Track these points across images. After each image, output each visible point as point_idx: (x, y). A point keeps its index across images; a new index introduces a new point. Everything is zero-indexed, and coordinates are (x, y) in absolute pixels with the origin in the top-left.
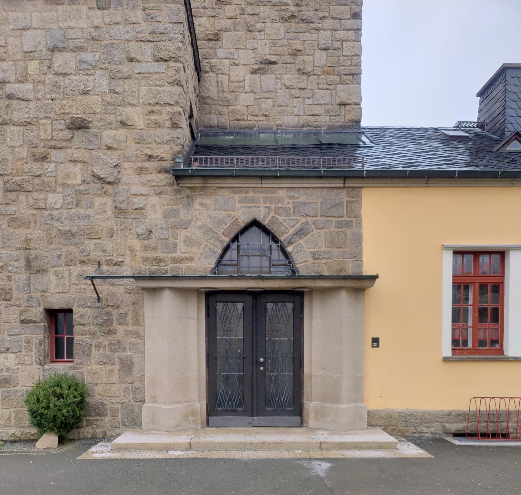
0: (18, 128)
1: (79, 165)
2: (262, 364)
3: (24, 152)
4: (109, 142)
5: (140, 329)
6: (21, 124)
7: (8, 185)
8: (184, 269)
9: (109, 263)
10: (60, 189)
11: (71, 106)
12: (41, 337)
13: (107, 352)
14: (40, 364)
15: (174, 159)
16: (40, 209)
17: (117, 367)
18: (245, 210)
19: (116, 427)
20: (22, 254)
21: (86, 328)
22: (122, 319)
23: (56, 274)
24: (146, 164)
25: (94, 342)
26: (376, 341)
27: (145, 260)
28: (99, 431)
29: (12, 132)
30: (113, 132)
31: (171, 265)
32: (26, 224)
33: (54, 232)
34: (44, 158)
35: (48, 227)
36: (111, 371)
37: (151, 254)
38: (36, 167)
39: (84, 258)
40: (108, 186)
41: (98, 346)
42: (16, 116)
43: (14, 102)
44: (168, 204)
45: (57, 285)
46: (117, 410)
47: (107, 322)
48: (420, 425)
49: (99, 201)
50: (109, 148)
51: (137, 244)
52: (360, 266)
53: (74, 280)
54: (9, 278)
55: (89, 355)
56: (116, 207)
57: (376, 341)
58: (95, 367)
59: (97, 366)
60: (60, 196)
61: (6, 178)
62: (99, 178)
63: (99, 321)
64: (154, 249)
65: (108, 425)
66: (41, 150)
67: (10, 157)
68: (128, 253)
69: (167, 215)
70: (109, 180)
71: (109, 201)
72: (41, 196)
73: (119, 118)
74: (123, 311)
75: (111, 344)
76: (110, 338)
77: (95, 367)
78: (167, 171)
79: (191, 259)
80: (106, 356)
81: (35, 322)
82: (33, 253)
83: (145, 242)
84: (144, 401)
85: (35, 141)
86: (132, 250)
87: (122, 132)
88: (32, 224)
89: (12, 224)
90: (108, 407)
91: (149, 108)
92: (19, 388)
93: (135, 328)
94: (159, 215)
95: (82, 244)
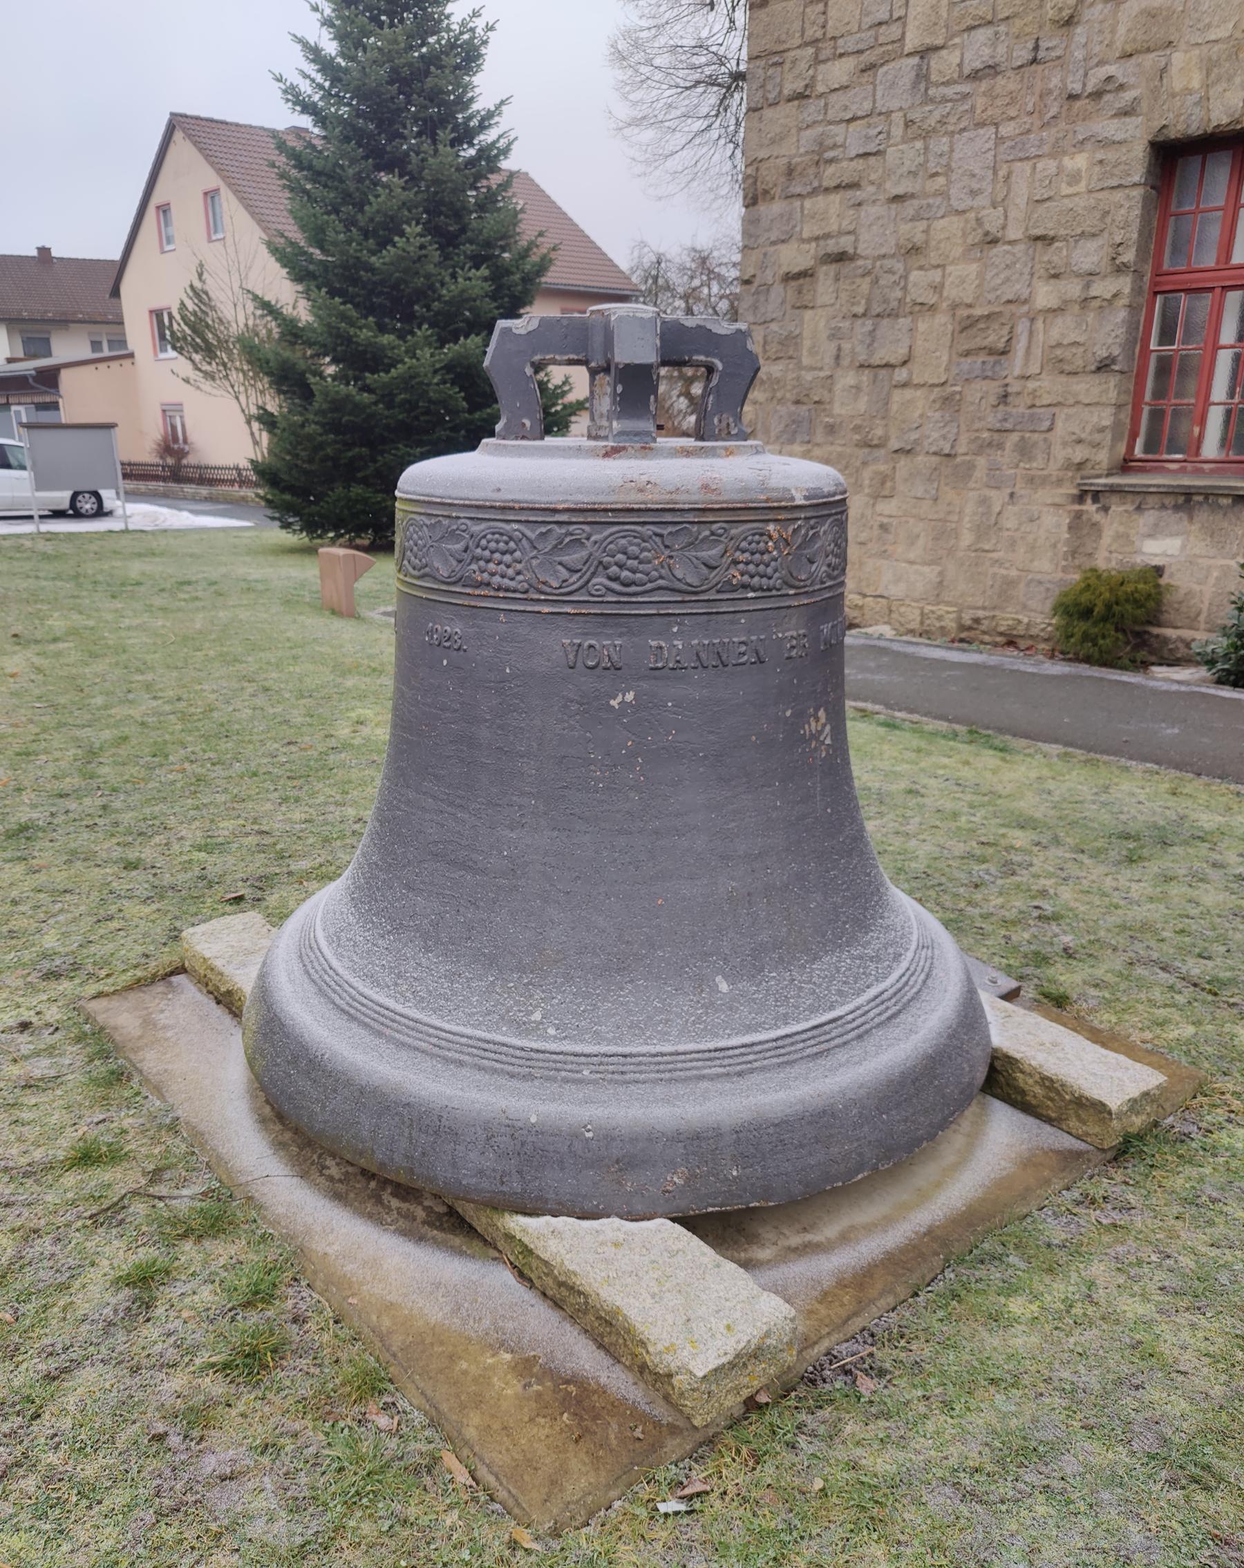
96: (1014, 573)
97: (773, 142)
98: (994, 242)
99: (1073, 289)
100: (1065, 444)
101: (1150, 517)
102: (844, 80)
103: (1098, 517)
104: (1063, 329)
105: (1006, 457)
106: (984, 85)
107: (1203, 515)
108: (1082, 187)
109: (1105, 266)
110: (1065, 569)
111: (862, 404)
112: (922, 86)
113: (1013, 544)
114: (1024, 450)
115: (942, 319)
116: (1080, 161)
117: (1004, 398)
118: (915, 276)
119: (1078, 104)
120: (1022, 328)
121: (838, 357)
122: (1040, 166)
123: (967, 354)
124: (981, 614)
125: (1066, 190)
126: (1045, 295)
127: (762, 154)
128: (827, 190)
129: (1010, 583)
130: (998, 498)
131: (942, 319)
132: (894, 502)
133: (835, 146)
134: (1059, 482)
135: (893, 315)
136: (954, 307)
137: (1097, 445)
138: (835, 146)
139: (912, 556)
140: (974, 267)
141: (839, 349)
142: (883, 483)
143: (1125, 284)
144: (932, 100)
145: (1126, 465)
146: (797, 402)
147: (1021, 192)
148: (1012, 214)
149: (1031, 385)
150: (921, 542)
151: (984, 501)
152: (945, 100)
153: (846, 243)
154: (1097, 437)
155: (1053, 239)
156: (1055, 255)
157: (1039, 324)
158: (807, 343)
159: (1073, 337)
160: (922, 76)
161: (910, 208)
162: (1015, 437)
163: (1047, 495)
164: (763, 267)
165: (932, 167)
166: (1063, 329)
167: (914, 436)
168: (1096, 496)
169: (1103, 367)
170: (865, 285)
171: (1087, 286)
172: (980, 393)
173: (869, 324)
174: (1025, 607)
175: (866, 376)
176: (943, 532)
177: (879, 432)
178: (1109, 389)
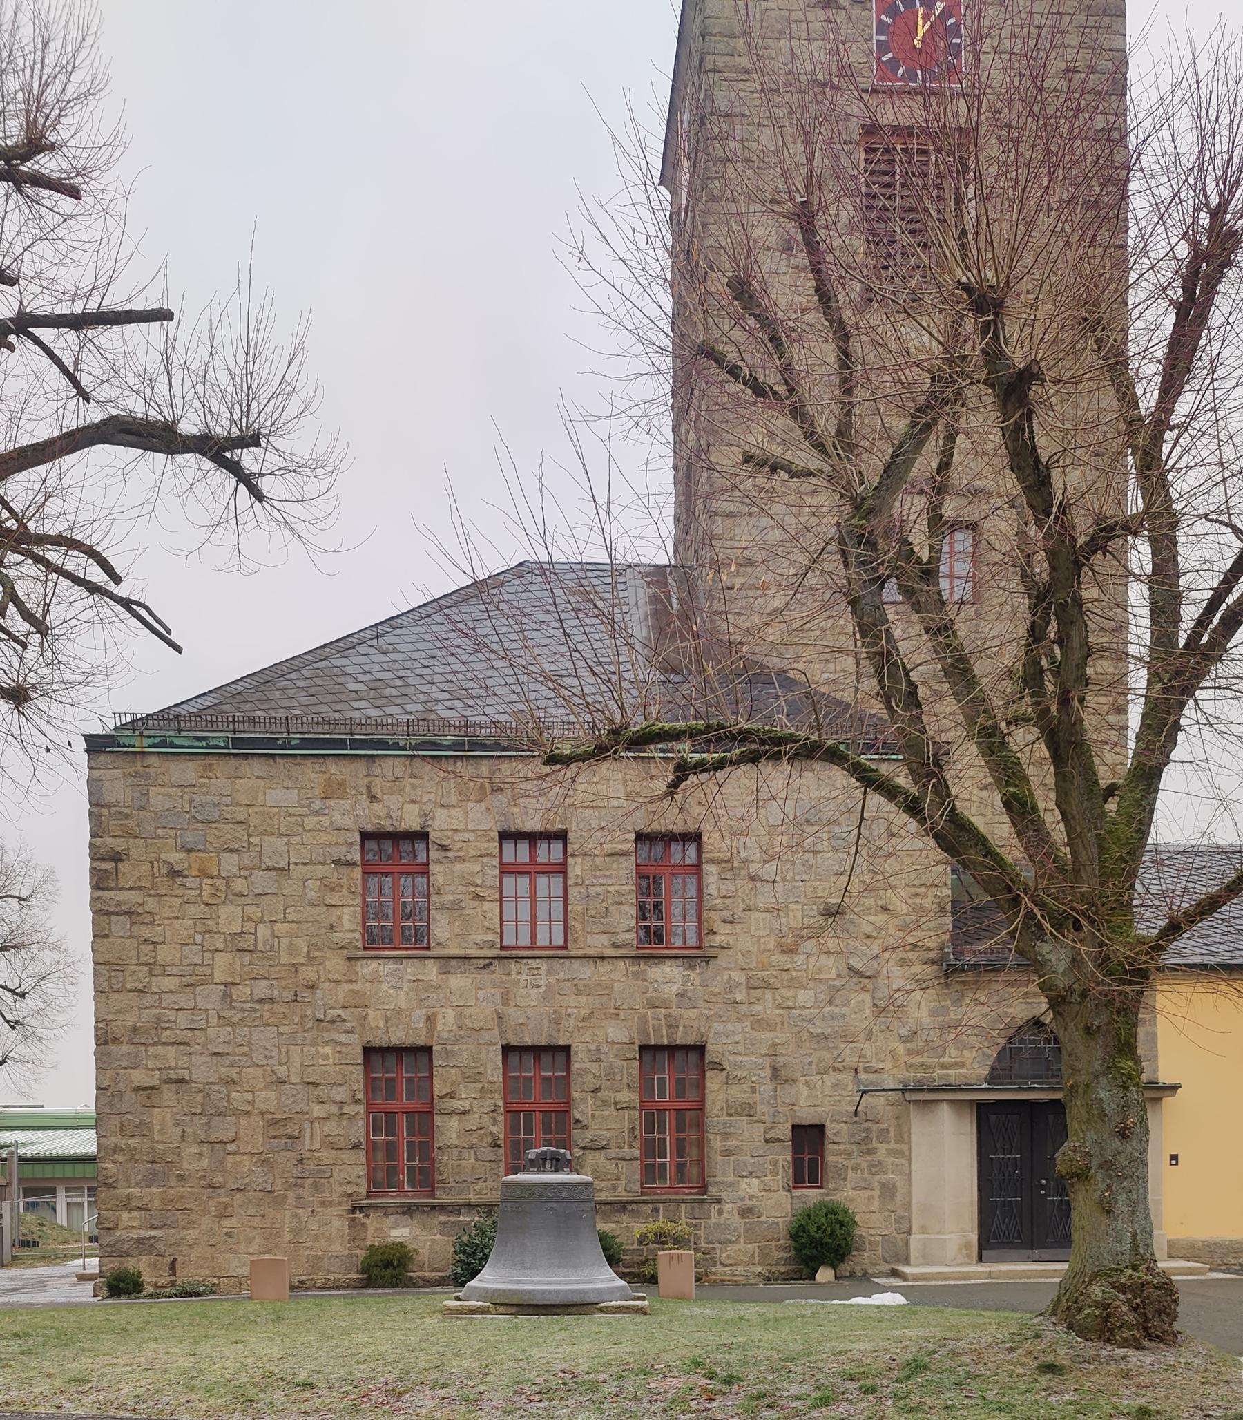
0: (764, 915)
1: (833, 957)
2: (1043, 1187)
3: (771, 943)
4: (868, 929)
5: (905, 1147)
6: (768, 911)
7: (752, 982)
8: (954, 1076)
9: (868, 1070)
10: (811, 985)
11: (824, 889)
12: (789, 1158)
13: (866, 1176)
14: (789, 1191)
15: (942, 949)
16: (789, 1008)
17: (877, 1193)
18: (1024, 1006)
19: (876, 1264)
20: (767, 1062)
21: (842, 1147)
22: (883, 1136)
23: (807, 1084)
24: (910, 955)
25: (850, 1163)
26: (1174, 1157)
27: (909, 1066)
28: (858, 1269)
29: (756, 919)
30: (873, 919)
31: (938, 1071)
32: (771, 1027)
33: (804, 1035)
34: (792, 951)
35: (798, 1029)
36: (871, 1198)
37: (918, 1059)
38: (782, 960)
39: (837, 1065)
40: (867, 981)
41: (856, 1168)
42: (761, 901)
43: (759, 884)
44: (935, 1000)
45: (809, 1097)
46: (877, 1245)
47: (867, 1140)
48: (1226, 1255)
49: (855, 998)
50: (869, 937)
51: (901, 1049)
52: (1155, 1071)
53: (827, 1091)
54: (753, 1090)
55: (845, 1179)
56: (875, 1005)
57: (1174, 1157)
58: (852, 1193)
59: (854, 1192)
60: (811, 993)
61: (750, 973)
62: (857, 972)
63: (858, 1138)
64: (920, 1053)
65: (866, 1261)
66: (790, 939)
67: (754, 949)
68: (889, 1057)
69: (933, 1013)
70: (869, 974)
71: (867, 997)
72: (790, 993)
73: (880, 903)
74: (884, 1126)
75: (871, 1166)
76: (869, 1158)
77: (852, 1193)
78: (933, 962)
79: (962, 1065)
80: (865, 1180)
81: (783, 1141)
82: (781, 1059)
83: (909, 1045)
84: (909, 1232)
85: (785, 930)
86: (892, 1053)
87: (881, 918)
88: (779, 1026)
89: (756, 1026)
90: (866, 1240)
91: (913, 890)
92: (763, 1219)
93: (898, 1147)
94: (924, 1013)
95: (836, 1048)
96: (320, 1253)
97: (119, 1011)
98: (284, 1082)
99: (334, 1109)
100: (341, 1184)
101: (392, 1218)
102: (173, 988)
103: (365, 1220)
104: (329, 1127)
105: (306, 1191)
106: (267, 1007)
107: (417, 1216)
108: (330, 1061)
109: (349, 1099)
110: (350, 1249)
111: (205, 1163)
112: (228, 1000)
113: (316, 1238)
114: (316, 1187)
115: (255, 1119)
116: (328, 1050)
117: (301, 1161)
118: (234, 1095)
119: (323, 1024)
120: (307, 1125)
121: (183, 1137)
122: (306, 1049)
123: (275, 1137)
124: (304, 1278)
125: (322, 1062)
126: (318, 1111)
127: (110, 1017)
128: (165, 1044)
129: (320, 1259)
130: (304, 1214)
131: (255, 1119)
132: (234, 1219)
133: (169, 1021)
134: (340, 1204)
135: (222, 1114)
136: (262, 1113)
137: (358, 1185)
138: (169, 1021)
139: (251, 1250)
140: (273, 1095)
141: (184, 1131)
142: (226, 1208)
143: (361, 1109)
144: (235, 1008)
145: (369, 1195)
146: (153, 1162)
147: (296, 1060)
148: (292, 1070)
149: (317, 1155)
150: (257, 1241)
151: (296, 1215)
152: (243, 1009)
153: (184, 1074)
154: (359, 1180)
155: (318, 1085)
156: (322, 1092)
157: (316, 1124)
158: (157, 1128)
159: (337, 1132)
160: (225, 996)
161: (226, 1060)
162: (310, 1181)
163: (334, 1210)
164: (116, 1081)
165: (239, 1041)
166: (329, 1127)
167: (245, 1181)
168: (361, 1209)
169: (356, 1146)
170: (200, 1097)
171: (341, 1108)
172: (286, 1159)
173: (205, 1119)
174: (329, 1271)
175: (205, 1148)
176: (271, 1235)
177: (221, 1179)
178: (361, 1156)
